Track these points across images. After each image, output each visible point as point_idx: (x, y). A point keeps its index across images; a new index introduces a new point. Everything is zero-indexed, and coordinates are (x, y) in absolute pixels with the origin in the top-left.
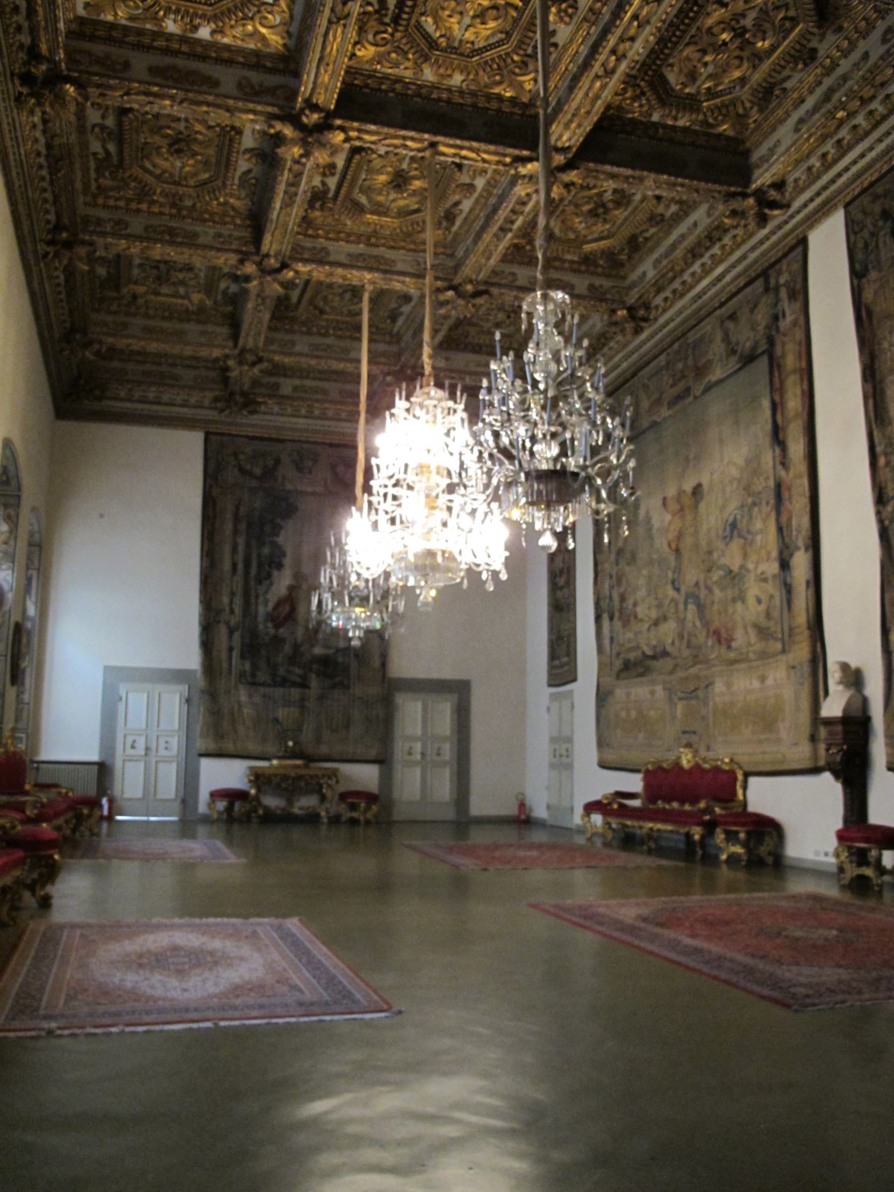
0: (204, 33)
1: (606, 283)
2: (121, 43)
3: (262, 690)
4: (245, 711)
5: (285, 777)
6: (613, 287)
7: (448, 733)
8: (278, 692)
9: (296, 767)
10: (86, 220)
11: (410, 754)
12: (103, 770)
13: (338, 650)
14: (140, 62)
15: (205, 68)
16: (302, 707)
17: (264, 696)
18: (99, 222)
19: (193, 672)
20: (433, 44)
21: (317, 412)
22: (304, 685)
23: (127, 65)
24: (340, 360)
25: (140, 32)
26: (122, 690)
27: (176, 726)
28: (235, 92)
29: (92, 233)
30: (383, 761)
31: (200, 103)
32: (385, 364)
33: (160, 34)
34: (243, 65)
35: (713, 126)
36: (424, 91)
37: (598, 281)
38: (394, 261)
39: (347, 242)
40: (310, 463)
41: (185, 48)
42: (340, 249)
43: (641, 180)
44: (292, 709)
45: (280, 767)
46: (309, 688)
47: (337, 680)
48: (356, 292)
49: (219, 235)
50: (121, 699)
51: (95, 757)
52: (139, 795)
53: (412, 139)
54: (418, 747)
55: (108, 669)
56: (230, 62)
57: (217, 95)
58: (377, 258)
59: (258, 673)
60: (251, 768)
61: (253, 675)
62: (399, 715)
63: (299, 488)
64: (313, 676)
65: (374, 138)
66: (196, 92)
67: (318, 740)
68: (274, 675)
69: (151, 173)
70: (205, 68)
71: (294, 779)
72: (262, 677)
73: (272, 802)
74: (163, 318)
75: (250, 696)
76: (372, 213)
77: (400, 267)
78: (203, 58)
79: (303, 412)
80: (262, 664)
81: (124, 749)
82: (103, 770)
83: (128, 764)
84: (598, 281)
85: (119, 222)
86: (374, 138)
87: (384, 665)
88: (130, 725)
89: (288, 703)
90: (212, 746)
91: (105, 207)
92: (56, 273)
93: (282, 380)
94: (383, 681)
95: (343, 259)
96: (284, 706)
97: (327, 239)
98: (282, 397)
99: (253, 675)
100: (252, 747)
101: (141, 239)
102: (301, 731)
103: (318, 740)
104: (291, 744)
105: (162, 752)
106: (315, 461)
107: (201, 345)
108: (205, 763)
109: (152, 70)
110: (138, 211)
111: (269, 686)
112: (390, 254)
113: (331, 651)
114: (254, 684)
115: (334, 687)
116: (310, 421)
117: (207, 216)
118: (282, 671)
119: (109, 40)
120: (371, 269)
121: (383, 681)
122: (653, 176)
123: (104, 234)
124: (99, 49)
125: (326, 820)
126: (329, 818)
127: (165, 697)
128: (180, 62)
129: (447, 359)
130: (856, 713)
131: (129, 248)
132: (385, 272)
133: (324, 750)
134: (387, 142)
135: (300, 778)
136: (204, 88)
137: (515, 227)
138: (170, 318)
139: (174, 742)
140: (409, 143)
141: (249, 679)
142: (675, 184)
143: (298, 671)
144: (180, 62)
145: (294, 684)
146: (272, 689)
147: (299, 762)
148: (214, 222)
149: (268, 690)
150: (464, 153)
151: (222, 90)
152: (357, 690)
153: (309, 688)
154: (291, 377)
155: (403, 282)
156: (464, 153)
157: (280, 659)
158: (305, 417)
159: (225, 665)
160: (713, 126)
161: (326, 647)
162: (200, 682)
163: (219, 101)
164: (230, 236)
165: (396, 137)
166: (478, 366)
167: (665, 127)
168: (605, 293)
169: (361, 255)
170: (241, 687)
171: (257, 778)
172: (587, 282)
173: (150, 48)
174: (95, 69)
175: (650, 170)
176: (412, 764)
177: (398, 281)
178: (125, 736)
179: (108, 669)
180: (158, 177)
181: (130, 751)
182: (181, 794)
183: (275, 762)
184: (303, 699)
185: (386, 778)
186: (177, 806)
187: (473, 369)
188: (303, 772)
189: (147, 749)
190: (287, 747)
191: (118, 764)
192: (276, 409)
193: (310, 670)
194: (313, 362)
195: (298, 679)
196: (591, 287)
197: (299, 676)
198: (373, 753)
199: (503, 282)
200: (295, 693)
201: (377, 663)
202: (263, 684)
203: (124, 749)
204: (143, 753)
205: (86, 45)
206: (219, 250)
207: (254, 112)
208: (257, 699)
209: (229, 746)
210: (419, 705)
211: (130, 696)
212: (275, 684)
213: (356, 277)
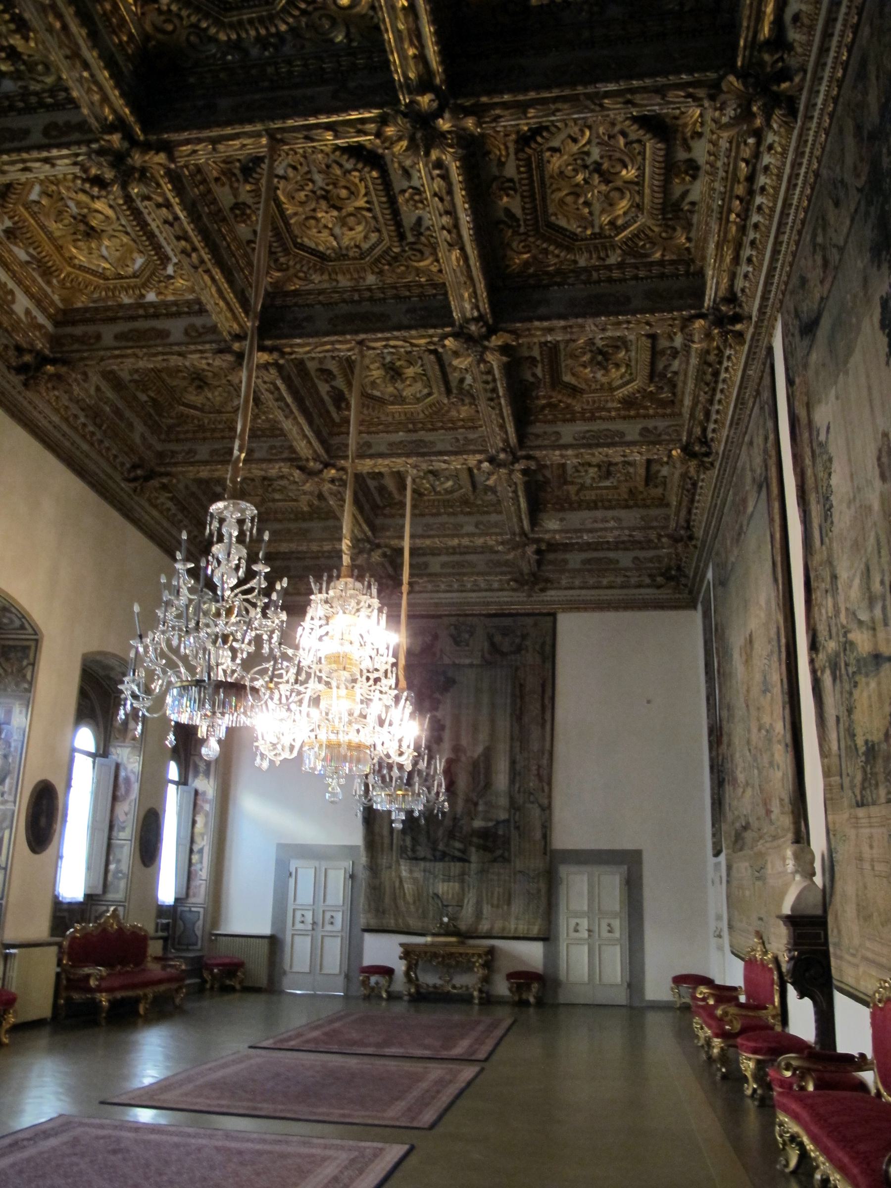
0: (151, 297)
1: (661, 424)
2: (92, 321)
3: (422, 864)
4: (406, 886)
5: (435, 955)
6: (670, 426)
7: (617, 908)
8: (439, 865)
9: (446, 944)
10: (161, 455)
11: (576, 931)
12: (274, 943)
13: (498, 823)
14: (108, 332)
15: (159, 324)
16: (462, 881)
17: (425, 871)
18: (174, 453)
19: (357, 847)
20: (322, 257)
21: (469, 586)
22: (464, 859)
23: (98, 337)
24: (453, 536)
25: (107, 309)
26: (293, 865)
27: (341, 903)
28: (184, 339)
29: (169, 464)
30: (547, 937)
31: (155, 355)
32: (496, 534)
33: (121, 306)
34: (188, 313)
35: (647, 256)
36: (345, 296)
37: (650, 424)
38: (432, 443)
39: (387, 432)
40: (467, 636)
41: (141, 312)
42: (381, 441)
43: (582, 327)
44: (451, 884)
45: (432, 944)
46: (469, 862)
47: (499, 852)
48: (400, 478)
49: (272, 447)
50: (291, 874)
51: (267, 931)
52: (307, 970)
53: (340, 342)
54: (584, 923)
55: (282, 847)
56: (178, 314)
57: (164, 345)
58: (421, 443)
59: (419, 848)
60: (401, 945)
61: (414, 850)
62: (563, 890)
63: (457, 662)
64: (473, 849)
65: (308, 349)
66: (149, 347)
67: (479, 915)
68: (434, 849)
69: (195, 408)
70: (159, 324)
71: (443, 957)
72: (422, 851)
73: (429, 979)
74: (290, 520)
75: (411, 871)
76: (393, 403)
77: (440, 447)
78: (156, 316)
79: (456, 586)
80: (423, 839)
81: (293, 925)
82: (274, 943)
83: (297, 938)
84: (650, 424)
85: (190, 451)
86: (308, 349)
87: (546, 837)
88: (299, 901)
89: (448, 879)
90: (373, 923)
91: (178, 440)
92: (159, 501)
93: (429, 559)
94: (545, 854)
95: (383, 449)
96: (444, 881)
97: (369, 433)
98: (430, 575)
99: (414, 850)
100: (414, 923)
101: (206, 463)
102: (462, 906)
103: (479, 915)
104: (446, 920)
105: (328, 927)
106: (471, 634)
107: (322, 540)
108: (368, 937)
109: (117, 337)
110: (204, 439)
111: (431, 861)
112: (429, 437)
113: (491, 824)
114: (416, 859)
115: (495, 860)
116: (464, 595)
117: (259, 433)
118: (441, 847)
119: (85, 321)
120: (408, 455)
121: (545, 854)
122: (590, 321)
123: (175, 464)
124: (79, 330)
125: (476, 1001)
126: (480, 998)
127: (331, 873)
128: (141, 324)
129: (561, 520)
130: (813, 908)
131: (198, 472)
132: (423, 455)
133: (484, 926)
134: (319, 349)
135: (451, 955)
136: (158, 341)
137: (501, 394)
138: (296, 520)
139: (339, 917)
140: (338, 346)
141: (410, 853)
142: (619, 323)
143: (458, 845)
144: (141, 324)
145: (455, 859)
146: (432, 864)
147: (453, 939)
148: (268, 436)
149: (428, 864)
150: (392, 343)
151: (172, 339)
152: (518, 864)
153: (469, 862)
154: (439, 555)
155: (445, 462)
156: (392, 343)
157: (440, 833)
158: (458, 591)
159: (387, 841)
160: (647, 256)
161: (486, 819)
162: (363, 859)
163: (167, 350)
164: (282, 446)
165: (326, 343)
166: (596, 521)
167: (597, 268)
168: (660, 435)
169: (401, 442)
170: (402, 862)
171: (408, 953)
172: (640, 426)
173: (113, 320)
174: (76, 346)
175: (584, 316)
176: (579, 942)
177: (440, 461)
178: (294, 910)
179: (282, 847)
180: (201, 410)
181: (299, 926)
182: (345, 968)
183: (429, 939)
184: (463, 874)
185: (551, 957)
186: (341, 981)
187: (589, 526)
188: (453, 950)
189: (314, 923)
190: (442, 923)
191: (288, 939)
192: (430, 587)
193: (471, 843)
194: (428, 542)
195: (457, 854)
196: (645, 431)
197: (459, 850)
198: (535, 931)
199: (546, 442)
200: (456, 868)
201: (538, 835)
202: (424, 859)
203: (293, 925)
204: (310, 927)
205: (69, 330)
206: (270, 461)
207: (201, 352)
208: (418, 875)
209: (392, 923)
210: (585, 878)
211: (299, 870)
212: (435, 859)
213: (399, 463)
